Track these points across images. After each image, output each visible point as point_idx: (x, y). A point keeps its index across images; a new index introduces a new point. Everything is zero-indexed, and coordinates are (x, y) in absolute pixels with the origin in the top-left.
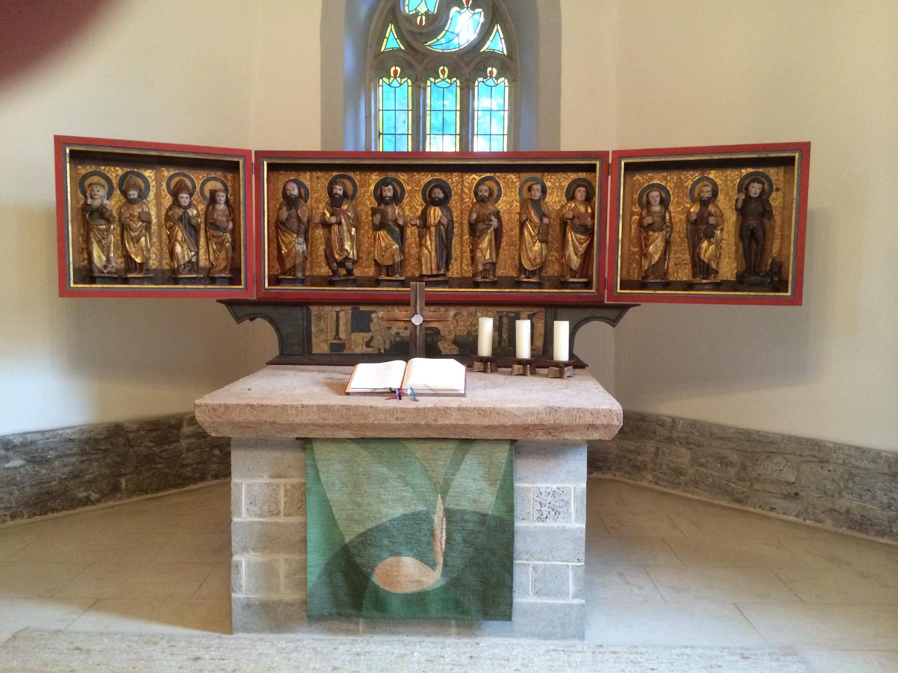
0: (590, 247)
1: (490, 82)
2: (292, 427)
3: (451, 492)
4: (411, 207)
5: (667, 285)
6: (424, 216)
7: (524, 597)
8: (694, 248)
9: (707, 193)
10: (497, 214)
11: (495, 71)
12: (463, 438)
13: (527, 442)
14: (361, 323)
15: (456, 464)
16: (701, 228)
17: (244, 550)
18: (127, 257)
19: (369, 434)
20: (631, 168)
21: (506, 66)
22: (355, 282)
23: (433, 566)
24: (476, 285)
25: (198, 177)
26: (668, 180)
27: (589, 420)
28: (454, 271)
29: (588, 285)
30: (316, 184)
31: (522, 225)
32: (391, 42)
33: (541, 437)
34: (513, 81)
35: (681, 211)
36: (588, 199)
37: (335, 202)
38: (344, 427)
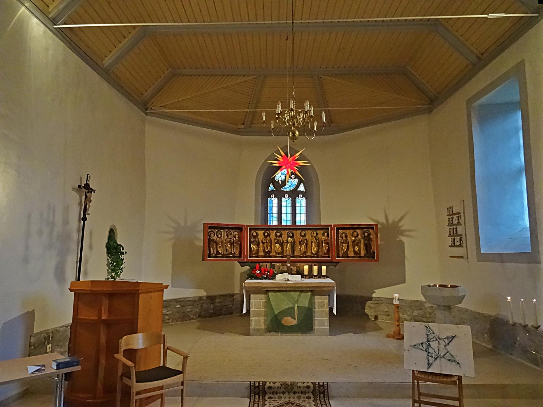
0: (329, 248)
1: (300, 199)
2: (265, 288)
3: (299, 302)
4: (284, 237)
5: (348, 257)
6: (287, 240)
7: (316, 327)
8: (354, 248)
9: (355, 234)
10: (306, 240)
11: (301, 196)
12: (300, 290)
13: (314, 291)
14: (273, 267)
15: (299, 296)
16: (356, 243)
17: (253, 316)
18: (218, 251)
19: (281, 289)
20: (338, 229)
21: (304, 194)
22: (270, 257)
23: (295, 319)
24: (301, 257)
25: (232, 231)
26: (348, 232)
27: (328, 285)
28: (295, 254)
29: (329, 257)
30: (261, 233)
31: (312, 242)
32: (271, 188)
33: (318, 289)
34: (306, 199)
35: (351, 239)
36: (328, 236)
37: (266, 237)
38: (276, 287)
